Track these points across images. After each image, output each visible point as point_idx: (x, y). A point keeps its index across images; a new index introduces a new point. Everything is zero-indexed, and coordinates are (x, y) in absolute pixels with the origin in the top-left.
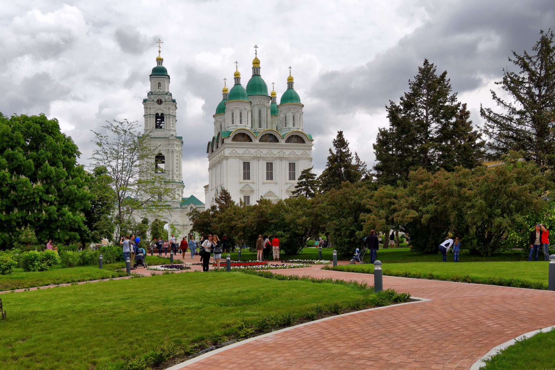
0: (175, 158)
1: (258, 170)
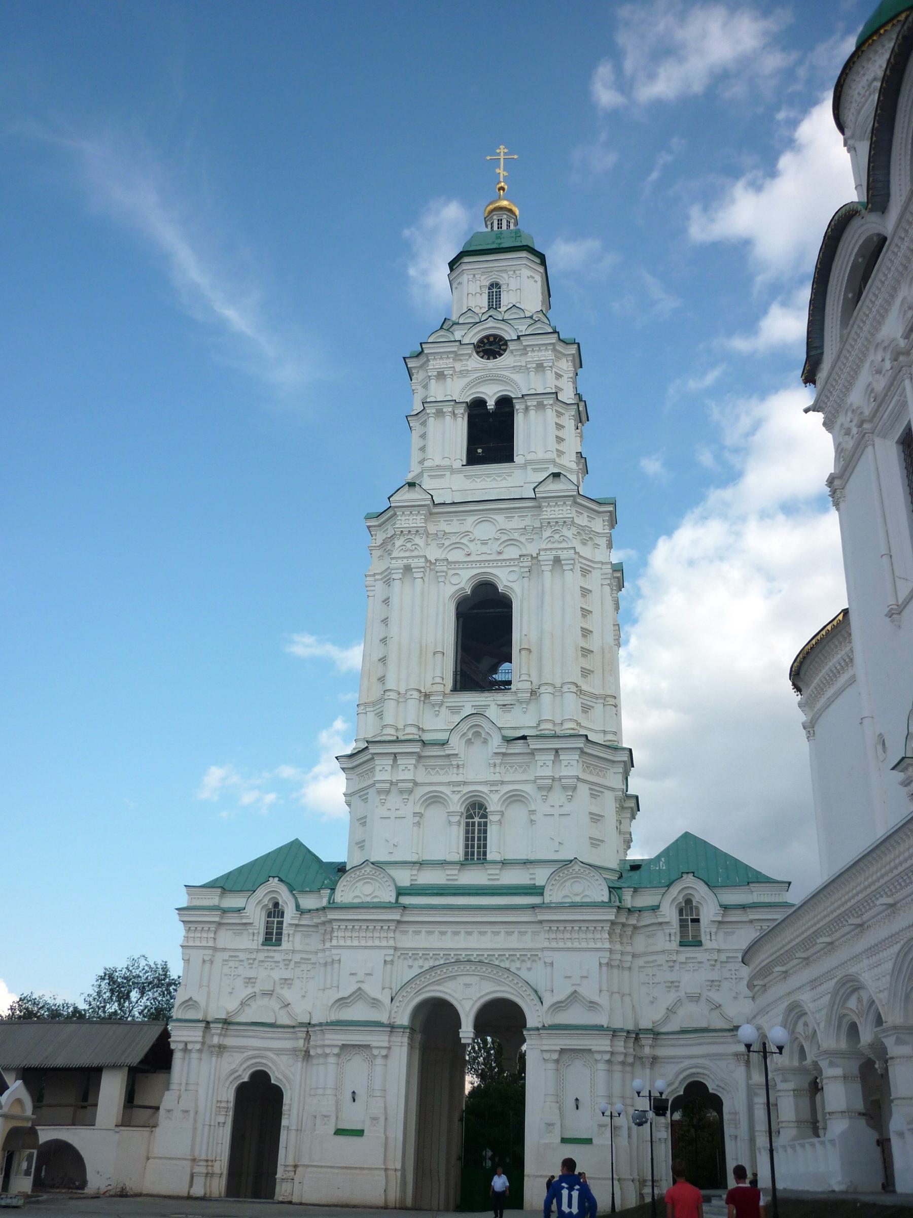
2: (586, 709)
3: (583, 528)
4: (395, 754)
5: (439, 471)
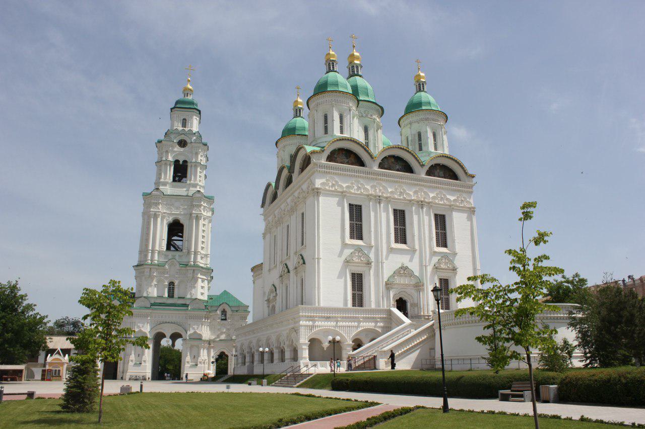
0: (201, 228)
1: (380, 222)
2: (202, 258)
3: (205, 207)
4: (150, 268)
5: (165, 184)
